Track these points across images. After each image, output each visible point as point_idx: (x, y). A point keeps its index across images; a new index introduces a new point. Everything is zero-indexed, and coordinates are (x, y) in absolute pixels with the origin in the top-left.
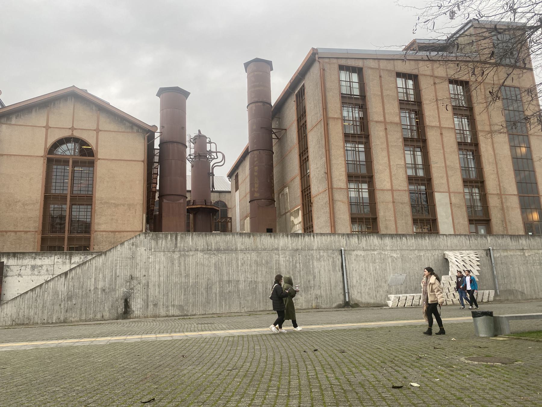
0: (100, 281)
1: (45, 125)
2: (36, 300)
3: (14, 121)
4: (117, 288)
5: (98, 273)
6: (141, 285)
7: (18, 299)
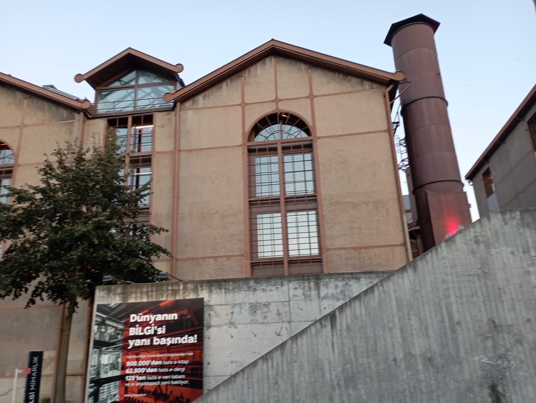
0: (415, 337)
1: (239, 102)
2: (276, 383)
4: (462, 353)
5: (406, 316)
6: (526, 346)
7: (239, 379)
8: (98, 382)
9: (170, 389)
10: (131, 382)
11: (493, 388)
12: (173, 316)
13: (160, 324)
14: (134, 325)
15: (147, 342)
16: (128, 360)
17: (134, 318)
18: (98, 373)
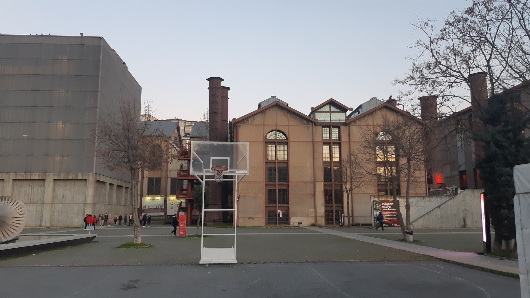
11: (464, 219)
12: (392, 204)
13: (389, 205)
14: (383, 205)
15: (387, 209)
17: (383, 204)
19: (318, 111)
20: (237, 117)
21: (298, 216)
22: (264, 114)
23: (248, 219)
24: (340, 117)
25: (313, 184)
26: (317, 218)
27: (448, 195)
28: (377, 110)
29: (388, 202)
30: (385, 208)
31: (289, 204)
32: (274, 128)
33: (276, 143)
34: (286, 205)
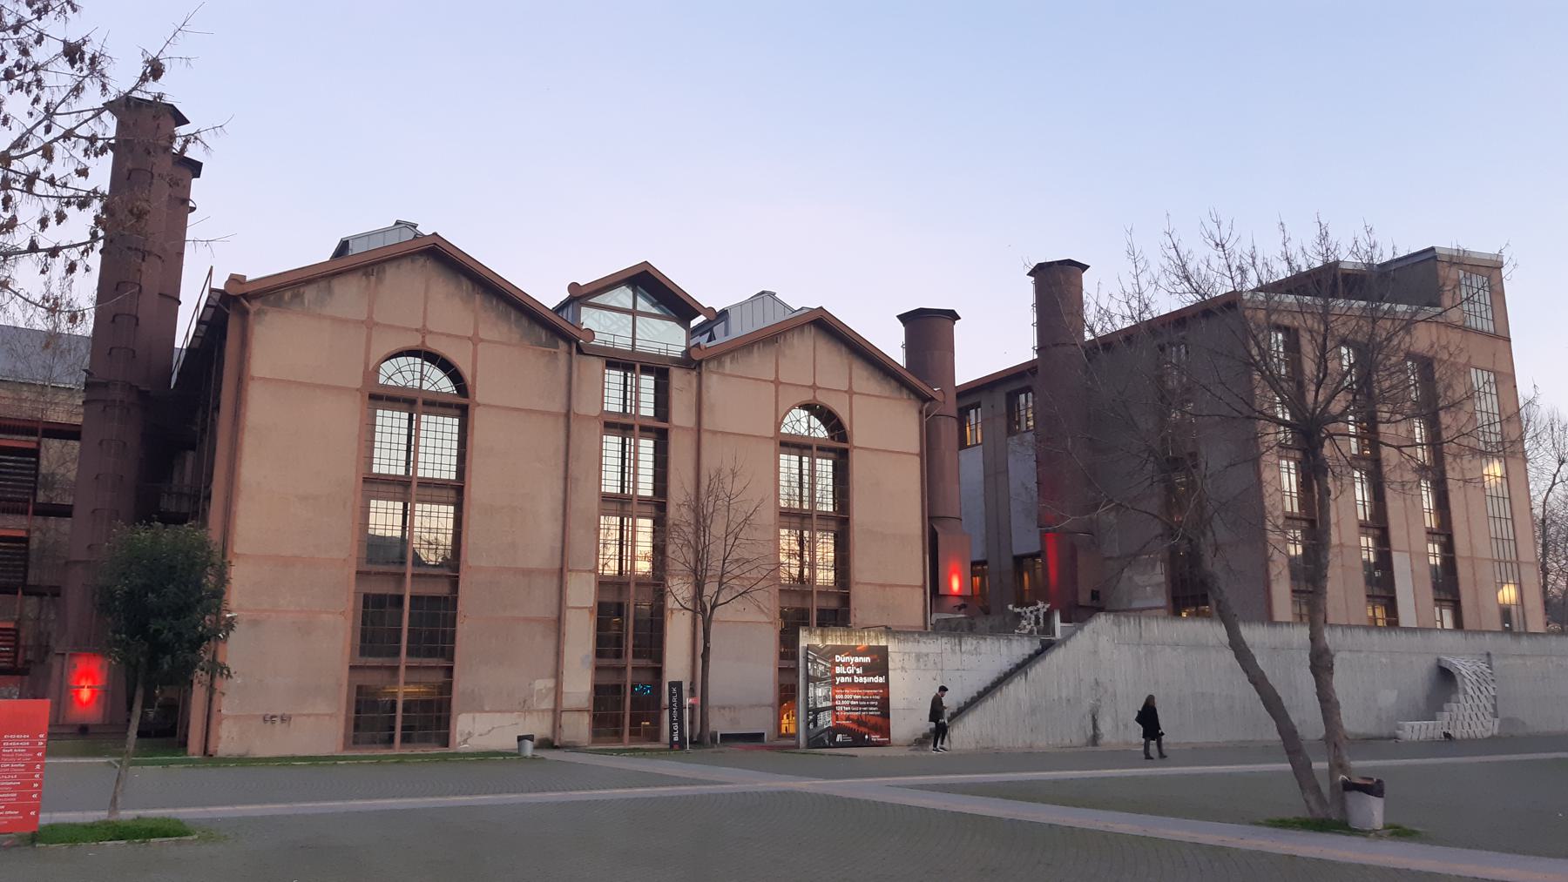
3: (728, 366)
8: (817, 711)
9: (868, 718)
10: (840, 711)
11: (1093, 717)
12: (867, 660)
13: (858, 665)
14: (839, 664)
15: (849, 679)
16: (836, 693)
17: (838, 658)
18: (815, 704)
19: (590, 301)
20: (254, 271)
21: (487, 709)
22: (373, 279)
23: (265, 720)
24: (665, 337)
25: (555, 580)
26: (563, 714)
27: (1026, 631)
28: (792, 329)
29: (853, 652)
30: (844, 675)
31: (452, 659)
32: (413, 342)
33: (411, 402)
34: (441, 662)
